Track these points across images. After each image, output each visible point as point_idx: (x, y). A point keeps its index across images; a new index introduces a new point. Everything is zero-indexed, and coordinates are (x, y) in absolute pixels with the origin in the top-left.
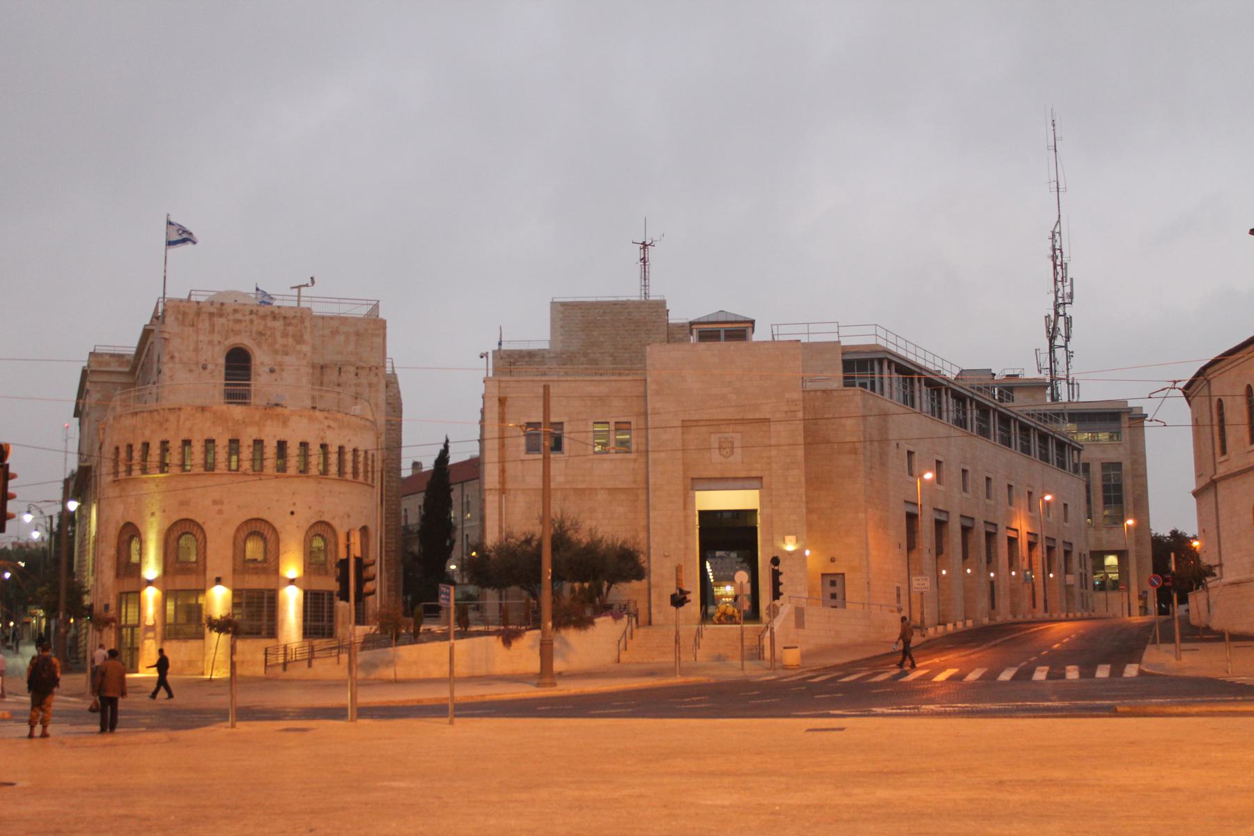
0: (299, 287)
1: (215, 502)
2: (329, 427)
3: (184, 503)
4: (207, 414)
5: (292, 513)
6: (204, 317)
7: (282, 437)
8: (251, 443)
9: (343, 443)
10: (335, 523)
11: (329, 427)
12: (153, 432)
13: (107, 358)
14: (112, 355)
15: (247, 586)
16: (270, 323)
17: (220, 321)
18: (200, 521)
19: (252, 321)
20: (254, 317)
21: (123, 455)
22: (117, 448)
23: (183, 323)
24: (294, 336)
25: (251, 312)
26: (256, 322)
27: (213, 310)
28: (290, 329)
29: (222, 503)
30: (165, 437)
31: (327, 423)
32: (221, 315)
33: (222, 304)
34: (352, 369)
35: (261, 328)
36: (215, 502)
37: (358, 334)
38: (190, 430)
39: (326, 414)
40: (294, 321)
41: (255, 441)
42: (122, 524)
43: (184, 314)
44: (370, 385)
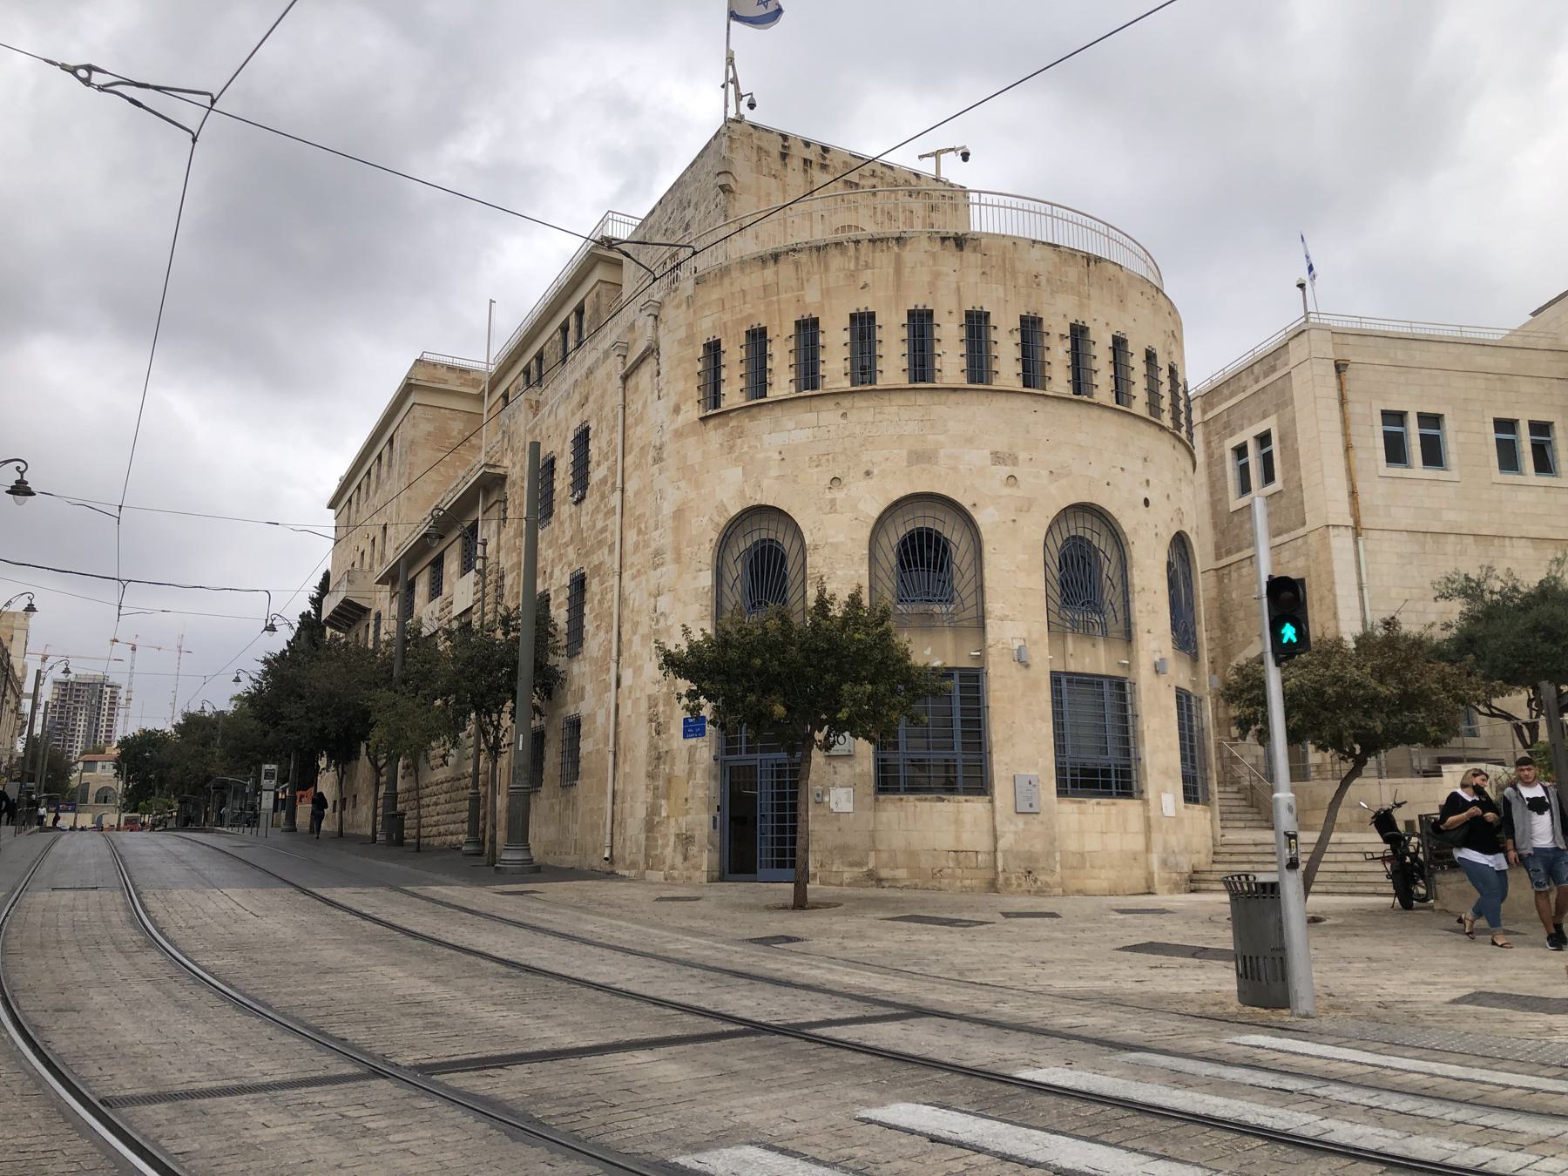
0: (937, 154)
1: (997, 458)
3: (921, 457)
4: (968, 254)
5: (1146, 502)
6: (795, 163)
7: (1117, 327)
12: (826, 292)
13: (442, 373)
14: (451, 368)
15: (1073, 666)
17: (820, 178)
18: (966, 502)
21: (734, 356)
22: (713, 350)
23: (758, 169)
27: (811, 154)
29: (1014, 460)
30: (863, 303)
32: (824, 167)
33: (825, 149)
35: (889, 206)
38: (932, 288)
41: (1073, 328)
42: (734, 511)
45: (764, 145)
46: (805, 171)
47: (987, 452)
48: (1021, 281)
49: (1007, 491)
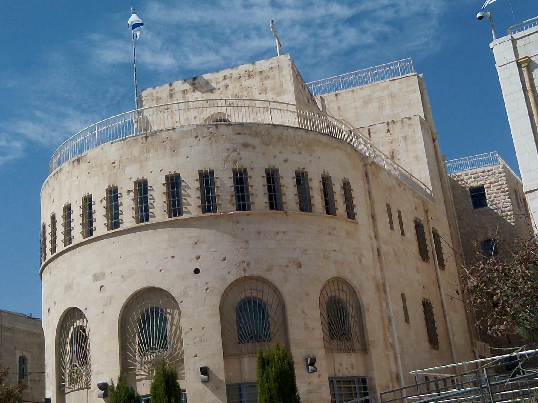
2: (246, 145)
5: (197, 271)
7: (171, 169)
8: (132, 187)
9: (276, 163)
10: (274, 277)
11: (246, 145)
16: (247, 82)
19: (226, 87)
20: (227, 81)
24: (273, 89)
25: (225, 78)
26: (230, 86)
28: (268, 83)
31: (240, 139)
34: (383, 127)
35: (236, 91)
36: (96, 278)
37: (392, 96)
39: (240, 129)
40: (271, 74)
43: (158, 99)
44: (405, 138)
45: (160, 95)
46: (184, 97)
47: (91, 276)
48: (106, 170)
49: (99, 295)
